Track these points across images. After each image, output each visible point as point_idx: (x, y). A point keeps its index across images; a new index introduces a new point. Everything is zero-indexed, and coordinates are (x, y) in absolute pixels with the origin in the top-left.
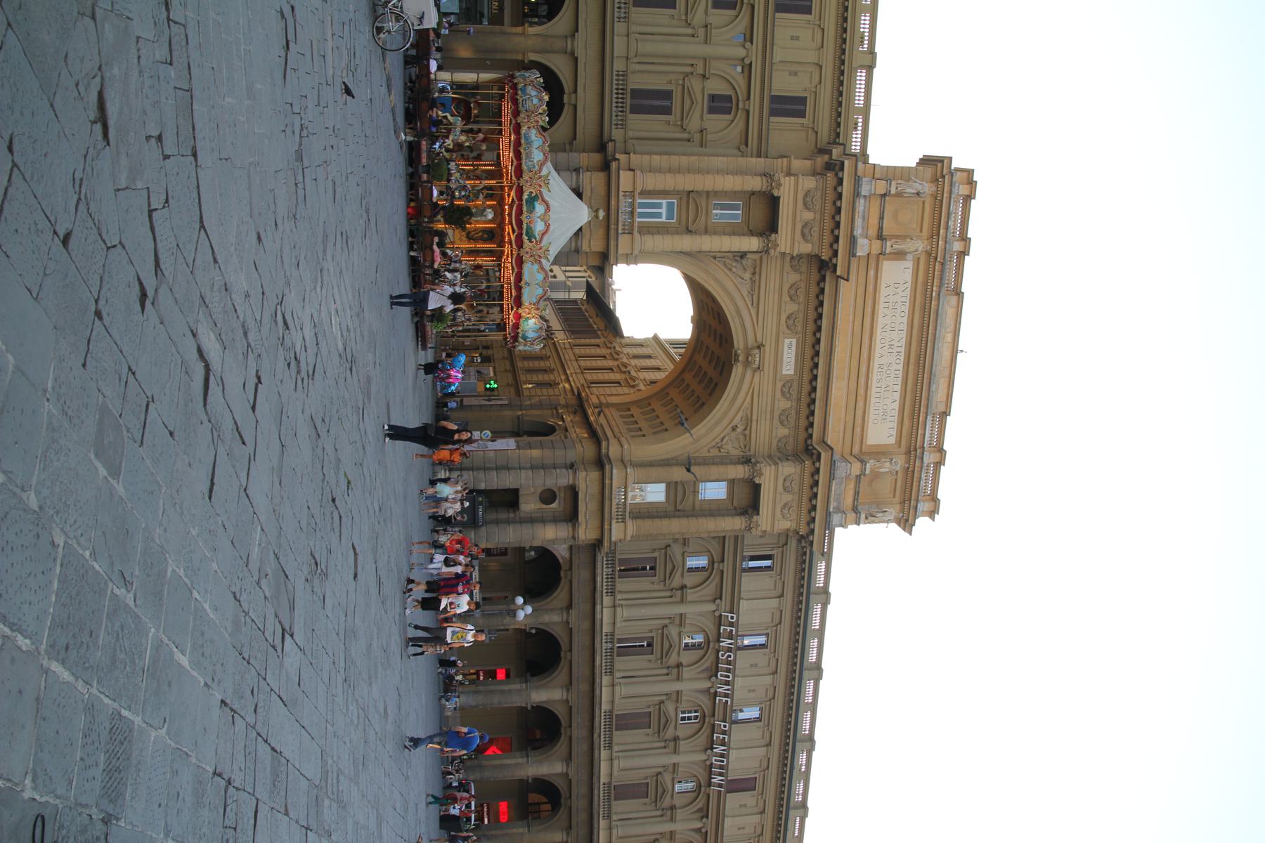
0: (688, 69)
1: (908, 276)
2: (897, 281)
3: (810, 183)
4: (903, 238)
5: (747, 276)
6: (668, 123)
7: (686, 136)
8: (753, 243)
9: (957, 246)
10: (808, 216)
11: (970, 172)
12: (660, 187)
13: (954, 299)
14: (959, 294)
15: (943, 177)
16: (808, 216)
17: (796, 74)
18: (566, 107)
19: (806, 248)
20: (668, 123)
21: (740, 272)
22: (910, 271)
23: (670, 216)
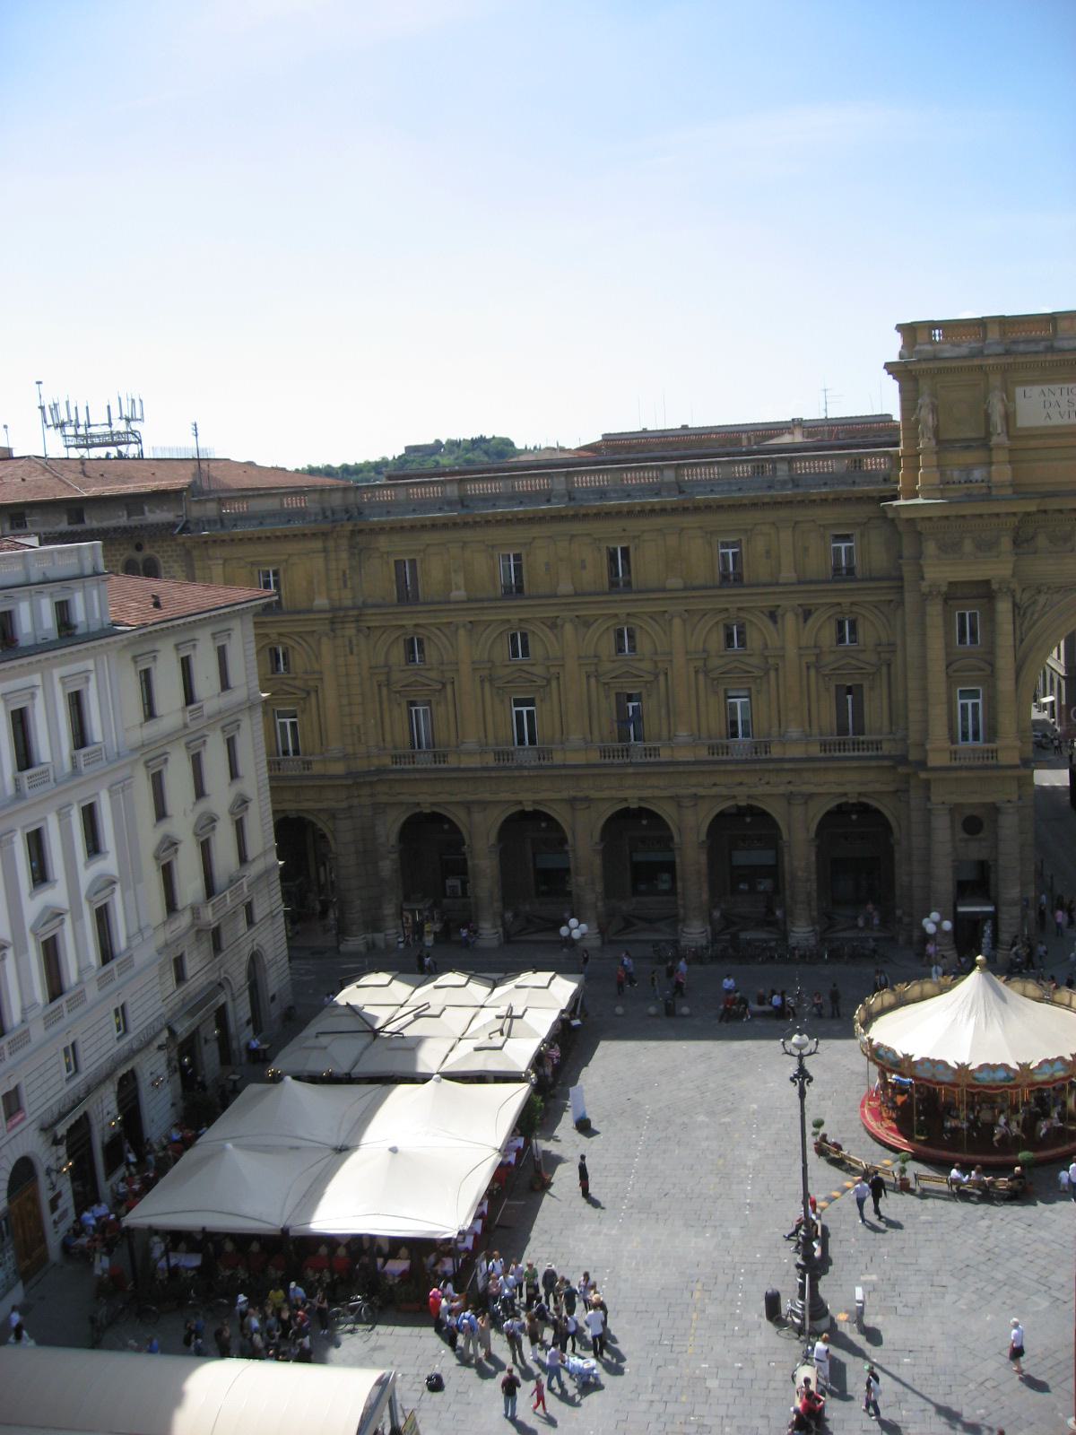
0: (813, 672)
1: (1034, 391)
2: (1040, 406)
3: (930, 548)
4: (988, 417)
5: (1042, 599)
6: (872, 688)
7: (884, 670)
8: (1004, 607)
9: (994, 334)
10: (968, 546)
11: (900, 328)
12: (944, 719)
13: (1063, 325)
14: (1053, 318)
15: (911, 371)
16: (968, 546)
17: (806, 549)
18: (864, 800)
19: (1006, 543)
20: (872, 688)
21: (1038, 608)
22: (1028, 389)
23: (974, 694)
